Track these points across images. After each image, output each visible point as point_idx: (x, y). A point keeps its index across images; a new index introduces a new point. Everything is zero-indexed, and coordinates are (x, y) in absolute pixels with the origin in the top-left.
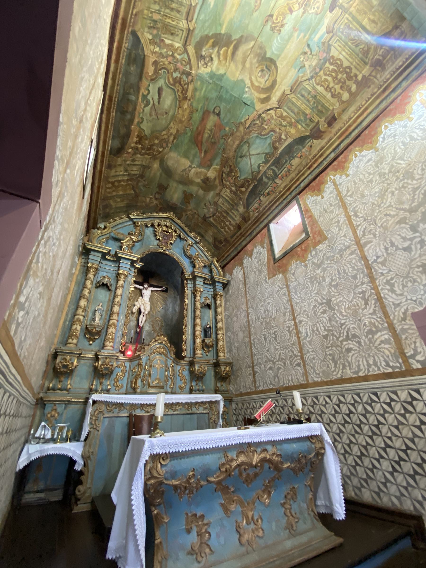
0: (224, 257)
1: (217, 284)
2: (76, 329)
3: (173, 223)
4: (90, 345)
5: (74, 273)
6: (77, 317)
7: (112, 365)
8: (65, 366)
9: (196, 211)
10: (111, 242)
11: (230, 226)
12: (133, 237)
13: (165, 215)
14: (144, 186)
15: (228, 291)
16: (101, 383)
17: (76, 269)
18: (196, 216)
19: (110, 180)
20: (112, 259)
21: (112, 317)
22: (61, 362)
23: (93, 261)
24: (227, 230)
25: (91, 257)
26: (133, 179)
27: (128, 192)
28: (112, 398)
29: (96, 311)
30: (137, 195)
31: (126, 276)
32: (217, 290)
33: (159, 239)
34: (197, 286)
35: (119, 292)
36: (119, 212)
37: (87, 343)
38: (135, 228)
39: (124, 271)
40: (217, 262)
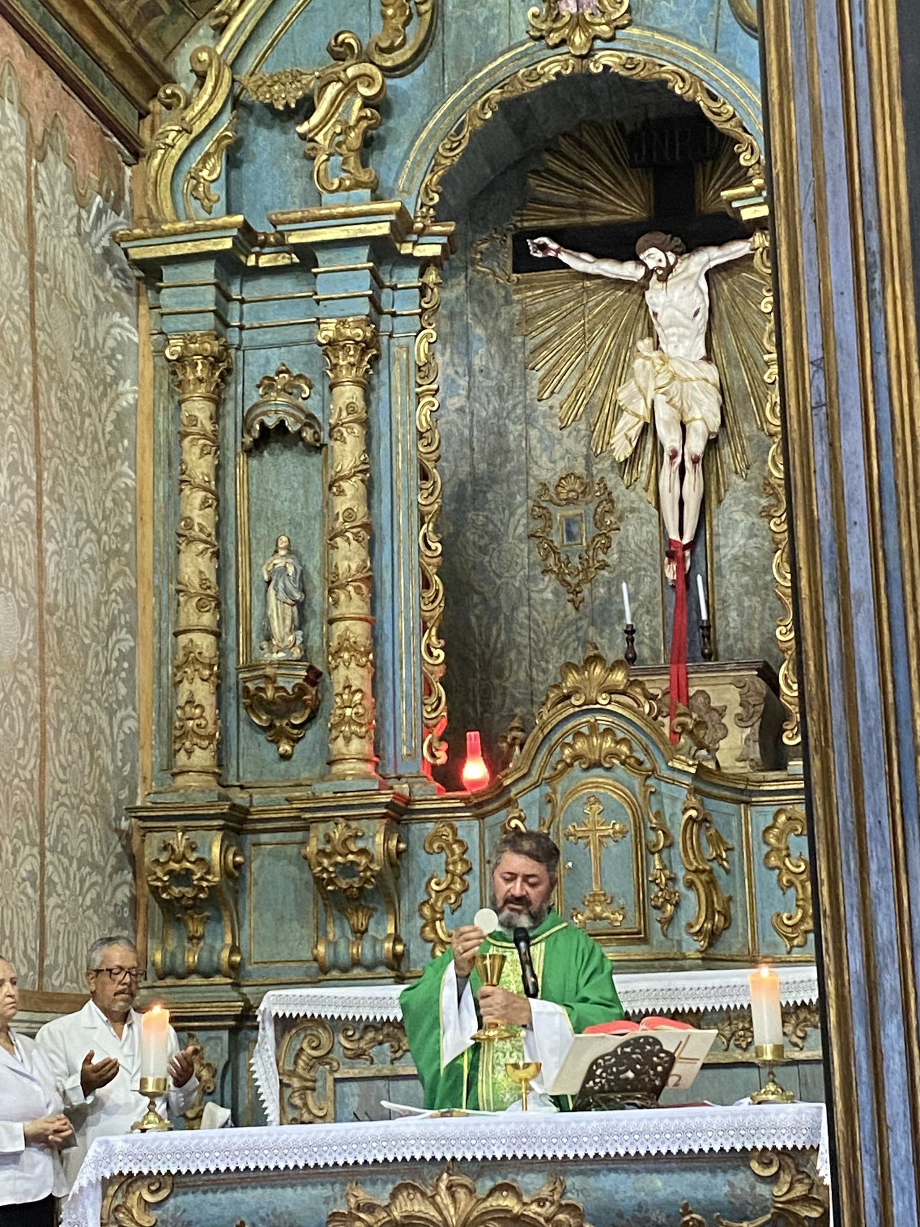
2: (189, 702)
4: (285, 757)
6: (183, 639)
7: (363, 852)
8: (183, 878)
10: (264, 141)
12: (351, 72)
16: (360, 933)
17: (136, 382)
20: (283, 260)
21: (336, 603)
22: (157, 861)
23: (182, 323)
25: (168, 299)
28: (347, 1003)
29: (269, 583)
31: (366, 345)
35: (347, 452)
37: (269, 753)
39: (343, 323)
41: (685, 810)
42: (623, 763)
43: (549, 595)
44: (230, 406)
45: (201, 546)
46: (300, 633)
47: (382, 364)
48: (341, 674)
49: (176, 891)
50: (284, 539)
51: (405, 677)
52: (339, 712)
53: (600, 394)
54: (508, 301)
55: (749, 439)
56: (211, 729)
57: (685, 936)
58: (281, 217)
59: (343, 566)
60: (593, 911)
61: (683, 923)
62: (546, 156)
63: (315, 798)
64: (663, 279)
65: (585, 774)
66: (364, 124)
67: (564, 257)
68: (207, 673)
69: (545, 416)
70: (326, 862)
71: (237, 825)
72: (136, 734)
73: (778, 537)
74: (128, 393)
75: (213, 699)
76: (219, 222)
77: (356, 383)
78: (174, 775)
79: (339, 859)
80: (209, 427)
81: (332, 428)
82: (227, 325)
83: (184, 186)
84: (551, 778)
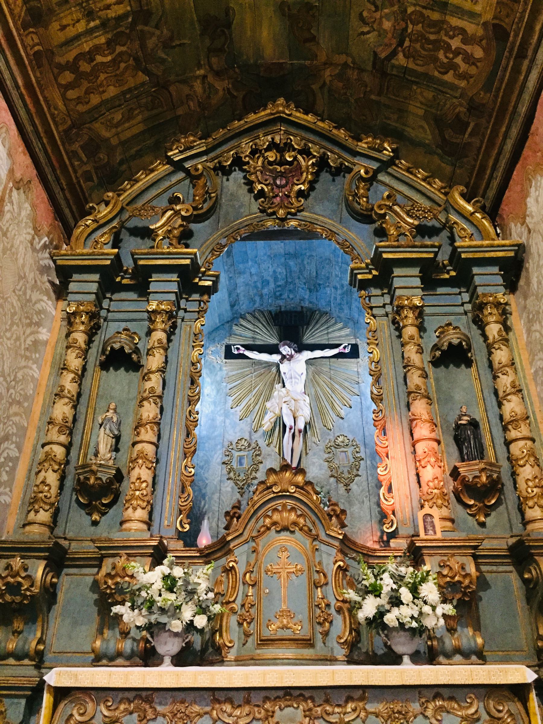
0: (488, 172)
1: (476, 270)
2: (43, 482)
3: (292, 130)
4: (95, 523)
5: (46, 343)
6: (47, 448)
8: (14, 589)
9: (342, 58)
11: (468, 48)
12: (178, 207)
13: (263, 115)
14: (167, 45)
15: (528, 283)
17: (49, 331)
18: (353, 75)
19: (61, 60)
21: (138, 434)
24: (463, 67)
25: (73, 287)
26: (123, 32)
27: (131, 83)
30: (162, 85)
31: (171, 315)
32: (480, 290)
33: (261, 194)
34: (398, 292)
35: (154, 362)
36: (139, 155)
37: (86, 520)
38: (194, 186)
40: (468, 201)
41: (336, 561)
42: (301, 529)
43: (229, 489)
44: (96, 343)
45: (67, 400)
46: (115, 453)
47: (177, 331)
48: (135, 473)
49: (8, 598)
50: (114, 404)
51: (171, 483)
52: (131, 493)
53: (257, 407)
54: (221, 369)
55: (320, 429)
56: (53, 500)
57: (336, 645)
58: (137, 251)
59: (145, 416)
60: (282, 622)
61: (335, 636)
62: (241, 320)
63: (110, 540)
64: (289, 360)
65: (277, 535)
66: (182, 229)
67: (247, 353)
68: (56, 467)
69: (233, 414)
70: (110, 582)
71: (58, 559)
72: (7, 506)
73: (377, 423)
74: (44, 334)
75: (57, 483)
76: (106, 251)
77: (164, 331)
78: (24, 526)
79: (119, 580)
80: (83, 346)
81: (149, 350)
82: (102, 308)
83: (90, 242)
84: (257, 537)
